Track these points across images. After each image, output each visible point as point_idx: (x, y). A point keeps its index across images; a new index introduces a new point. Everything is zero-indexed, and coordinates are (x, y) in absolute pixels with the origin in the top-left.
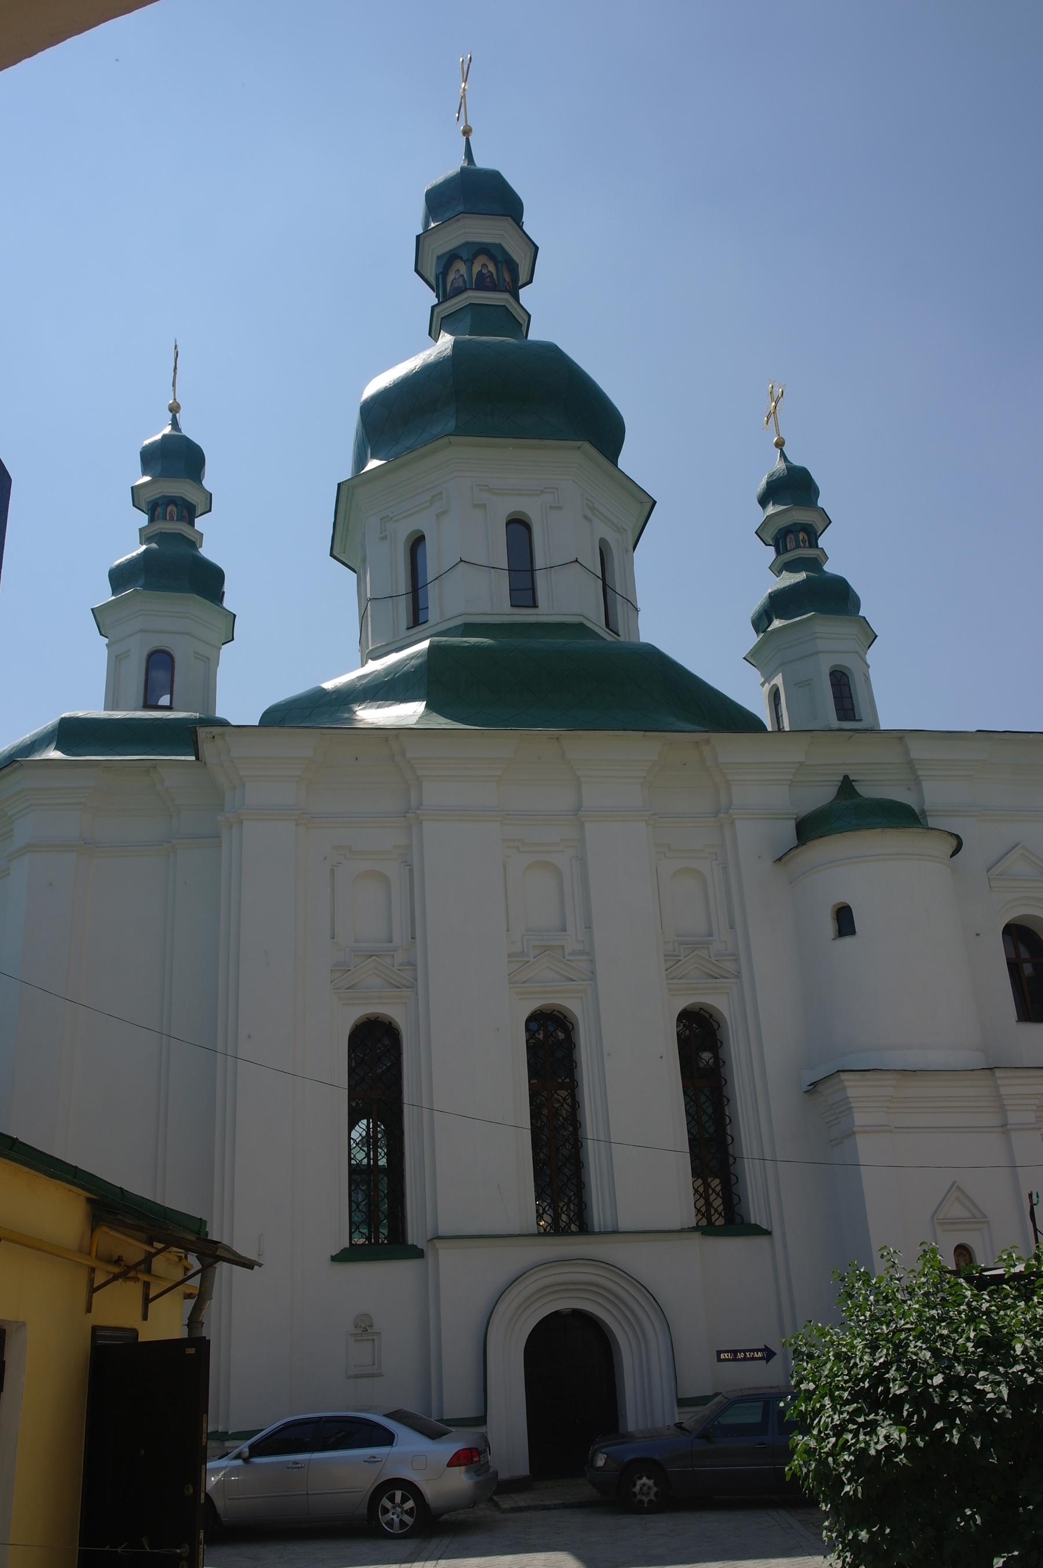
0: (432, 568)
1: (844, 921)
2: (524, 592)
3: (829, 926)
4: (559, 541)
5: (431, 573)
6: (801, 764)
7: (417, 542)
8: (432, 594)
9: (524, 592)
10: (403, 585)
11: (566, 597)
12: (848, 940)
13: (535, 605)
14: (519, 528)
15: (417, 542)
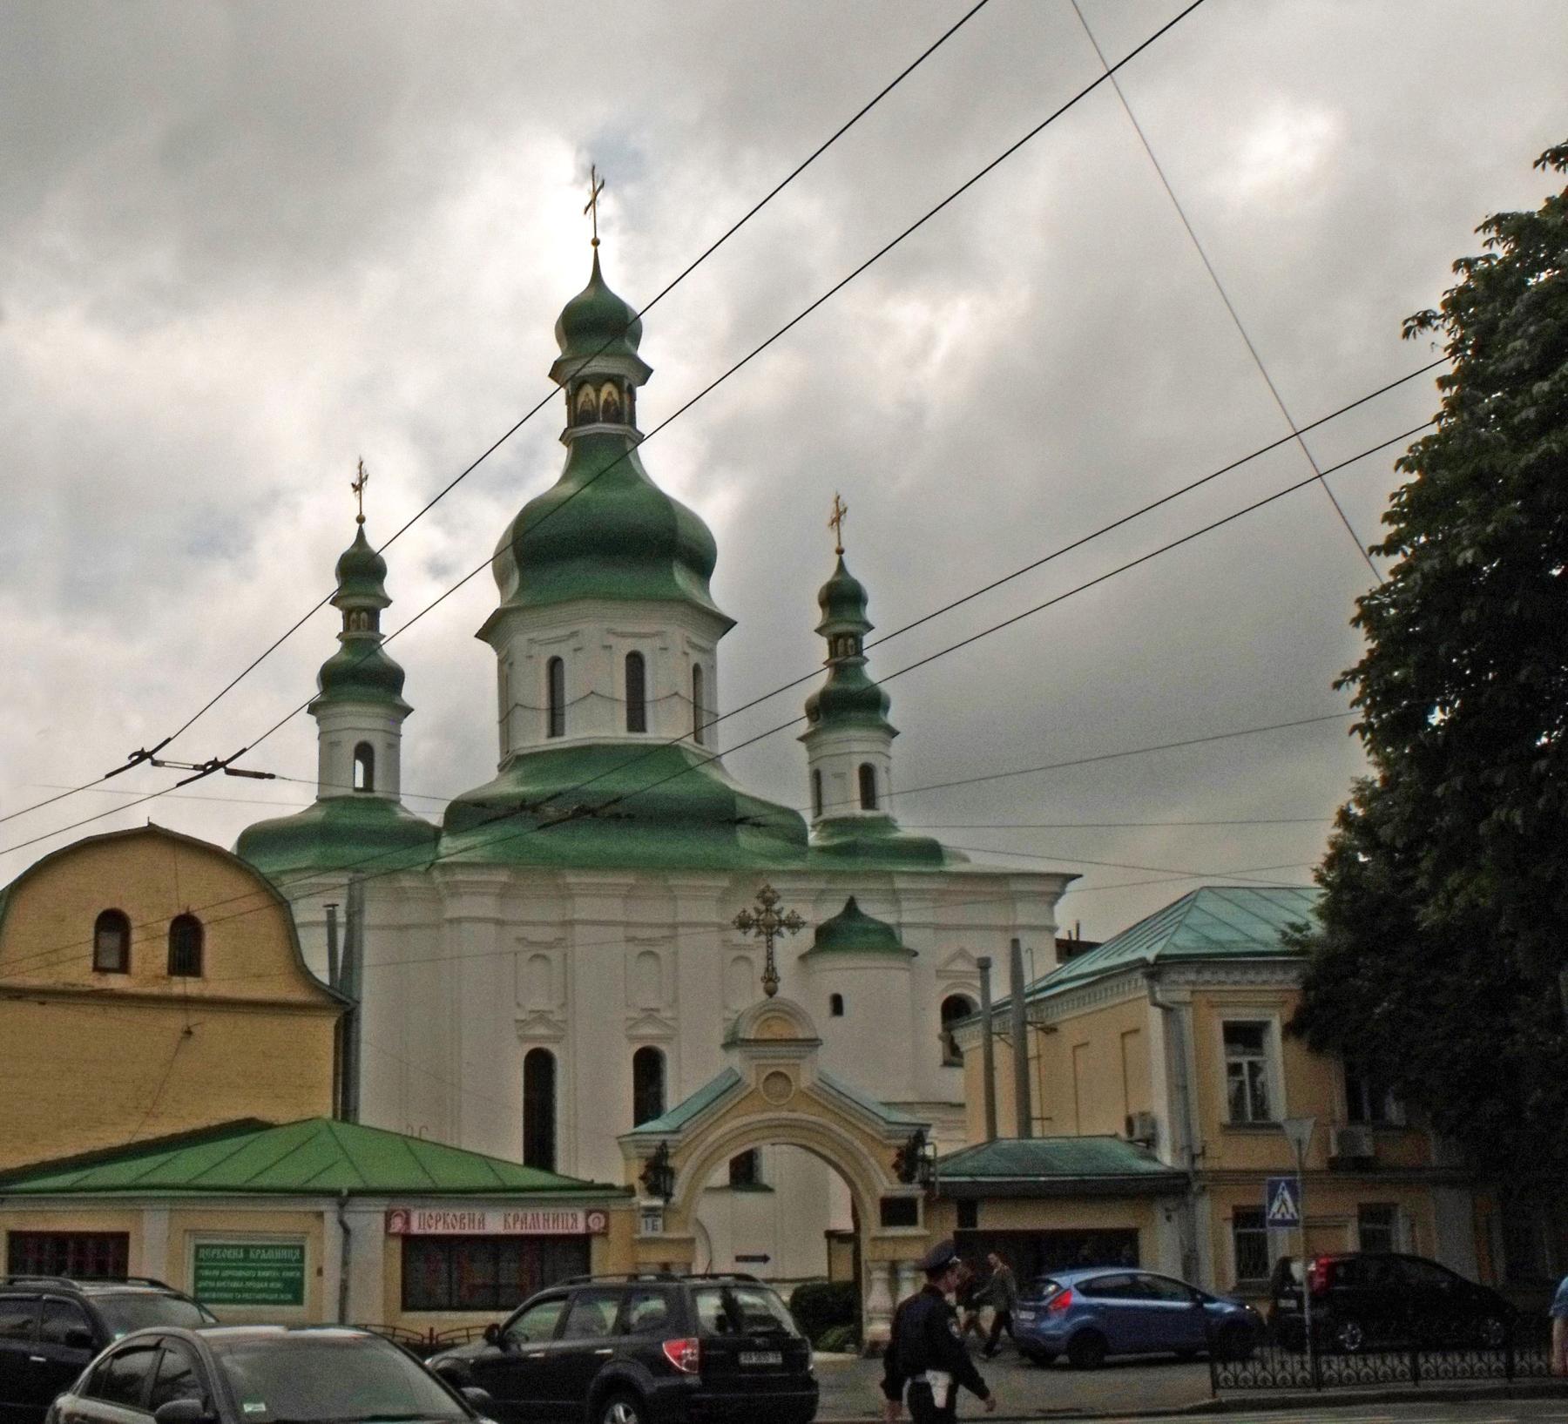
0: (570, 693)
1: (837, 1005)
2: (636, 721)
3: (827, 1007)
4: (665, 677)
5: (568, 699)
6: (823, 891)
7: (555, 664)
8: (570, 716)
9: (636, 721)
10: (543, 702)
11: (667, 725)
12: (838, 1019)
13: (642, 729)
14: (635, 663)
15: (555, 664)
